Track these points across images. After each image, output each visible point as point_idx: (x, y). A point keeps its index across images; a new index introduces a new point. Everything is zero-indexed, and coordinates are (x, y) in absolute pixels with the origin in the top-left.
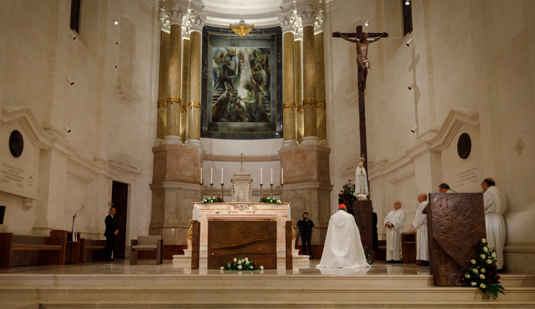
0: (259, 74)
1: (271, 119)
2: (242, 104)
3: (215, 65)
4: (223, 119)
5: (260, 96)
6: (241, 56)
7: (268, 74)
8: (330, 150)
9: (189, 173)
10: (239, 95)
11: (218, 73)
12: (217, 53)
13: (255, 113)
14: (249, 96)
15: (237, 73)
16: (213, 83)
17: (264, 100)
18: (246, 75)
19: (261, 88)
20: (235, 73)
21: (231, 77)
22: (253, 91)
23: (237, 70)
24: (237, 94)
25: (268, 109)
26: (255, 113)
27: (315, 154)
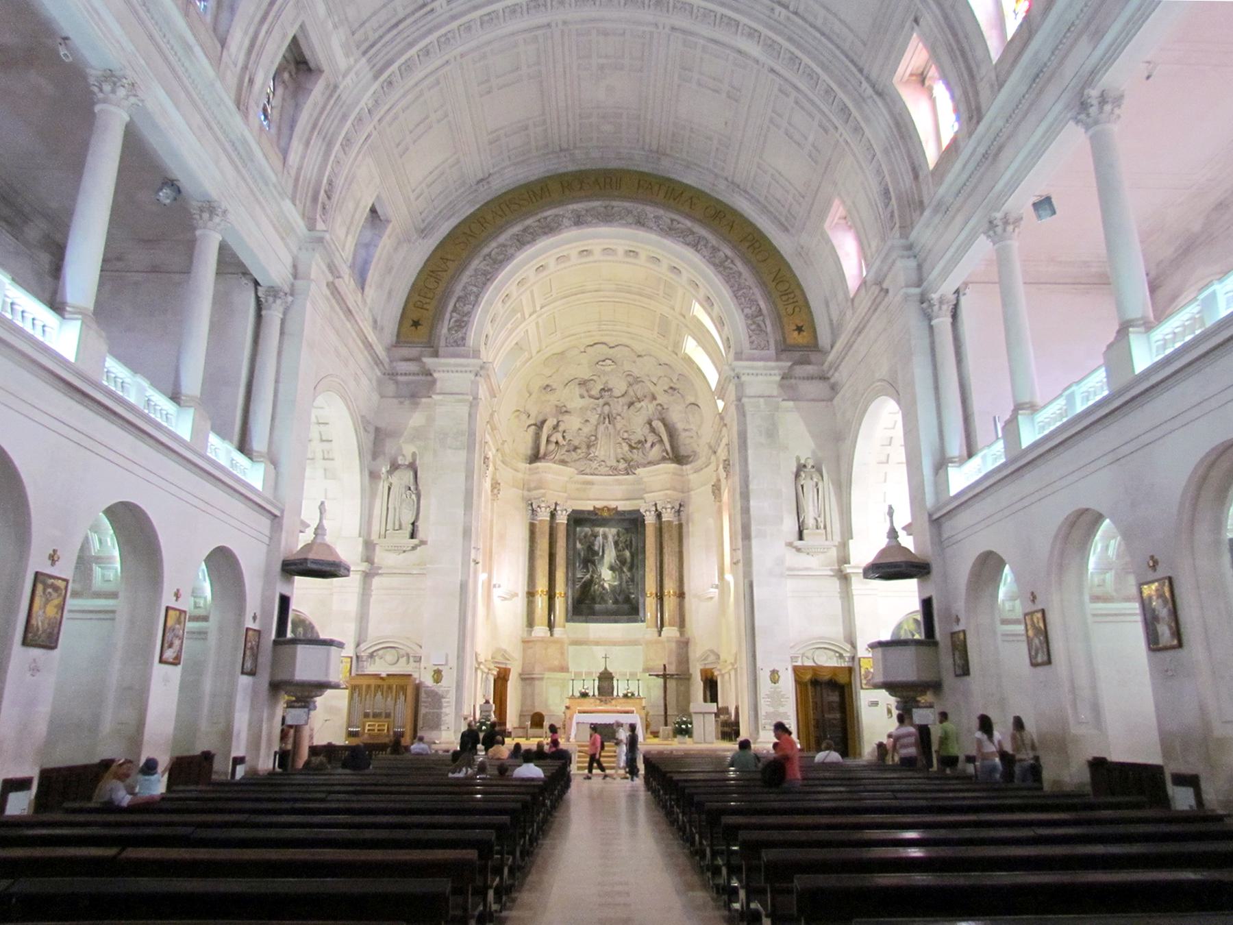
0: (623, 555)
1: (634, 601)
2: (606, 585)
3: (579, 546)
4: (587, 602)
5: (624, 578)
6: (605, 537)
7: (632, 556)
8: (689, 639)
9: (556, 663)
10: (603, 576)
11: (582, 554)
12: (581, 533)
13: (619, 595)
14: (613, 578)
15: (601, 554)
16: (578, 564)
17: (627, 582)
18: (610, 556)
19: (625, 570)
20: (598, 554)
21: (596, 558)
22: (617, 573)
23: (601, 550)
24: (600, 575)
25: (632, 591)
26: (619, 595)
27: (674, 645)
